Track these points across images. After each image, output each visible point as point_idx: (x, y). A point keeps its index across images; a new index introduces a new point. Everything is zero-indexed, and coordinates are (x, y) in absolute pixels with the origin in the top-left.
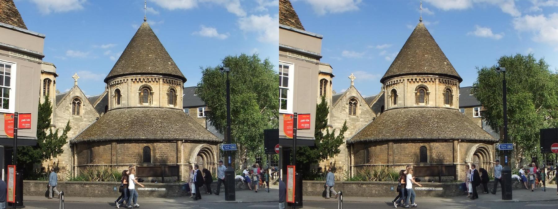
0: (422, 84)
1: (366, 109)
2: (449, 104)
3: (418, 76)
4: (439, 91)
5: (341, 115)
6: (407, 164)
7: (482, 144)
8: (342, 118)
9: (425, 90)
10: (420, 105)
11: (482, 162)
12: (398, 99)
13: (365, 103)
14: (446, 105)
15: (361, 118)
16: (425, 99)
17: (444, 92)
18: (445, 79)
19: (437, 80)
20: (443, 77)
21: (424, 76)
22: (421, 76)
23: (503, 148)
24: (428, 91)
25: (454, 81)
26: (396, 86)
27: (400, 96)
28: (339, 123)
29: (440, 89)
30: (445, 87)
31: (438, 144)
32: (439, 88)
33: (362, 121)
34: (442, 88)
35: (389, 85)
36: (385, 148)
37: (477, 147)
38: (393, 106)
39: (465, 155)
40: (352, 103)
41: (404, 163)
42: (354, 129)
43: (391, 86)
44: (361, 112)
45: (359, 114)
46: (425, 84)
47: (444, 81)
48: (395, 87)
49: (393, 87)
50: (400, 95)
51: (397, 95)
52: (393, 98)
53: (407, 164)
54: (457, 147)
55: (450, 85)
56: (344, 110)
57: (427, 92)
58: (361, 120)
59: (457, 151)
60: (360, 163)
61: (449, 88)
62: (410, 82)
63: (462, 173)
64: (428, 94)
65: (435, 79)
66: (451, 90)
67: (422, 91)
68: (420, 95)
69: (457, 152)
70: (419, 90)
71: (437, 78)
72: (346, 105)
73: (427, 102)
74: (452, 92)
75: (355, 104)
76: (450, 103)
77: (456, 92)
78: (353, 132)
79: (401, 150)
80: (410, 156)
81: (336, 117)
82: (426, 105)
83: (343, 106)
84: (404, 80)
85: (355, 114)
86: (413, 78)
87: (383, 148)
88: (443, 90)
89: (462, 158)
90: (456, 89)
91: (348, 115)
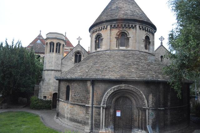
4: (110, 36)
7: (124, 85)
19: (109, 27)
28: (66, 68)
29: (113, 34)
30: (118, 32)
32: (110, 33)
34: (115, 32)
37: (114, 88)
39: (101, 97)
46: (100, 32)
47: (116, 26)
54: (89, 88)
56: (71, 60)
61: (123, 31)
64: (102, 39)
65: (107, 26)
68: (98, 42)
69: (89, 93)
74: (128, 34)
81: (64, 65)
85: (80, 60)
89: (97, 100)
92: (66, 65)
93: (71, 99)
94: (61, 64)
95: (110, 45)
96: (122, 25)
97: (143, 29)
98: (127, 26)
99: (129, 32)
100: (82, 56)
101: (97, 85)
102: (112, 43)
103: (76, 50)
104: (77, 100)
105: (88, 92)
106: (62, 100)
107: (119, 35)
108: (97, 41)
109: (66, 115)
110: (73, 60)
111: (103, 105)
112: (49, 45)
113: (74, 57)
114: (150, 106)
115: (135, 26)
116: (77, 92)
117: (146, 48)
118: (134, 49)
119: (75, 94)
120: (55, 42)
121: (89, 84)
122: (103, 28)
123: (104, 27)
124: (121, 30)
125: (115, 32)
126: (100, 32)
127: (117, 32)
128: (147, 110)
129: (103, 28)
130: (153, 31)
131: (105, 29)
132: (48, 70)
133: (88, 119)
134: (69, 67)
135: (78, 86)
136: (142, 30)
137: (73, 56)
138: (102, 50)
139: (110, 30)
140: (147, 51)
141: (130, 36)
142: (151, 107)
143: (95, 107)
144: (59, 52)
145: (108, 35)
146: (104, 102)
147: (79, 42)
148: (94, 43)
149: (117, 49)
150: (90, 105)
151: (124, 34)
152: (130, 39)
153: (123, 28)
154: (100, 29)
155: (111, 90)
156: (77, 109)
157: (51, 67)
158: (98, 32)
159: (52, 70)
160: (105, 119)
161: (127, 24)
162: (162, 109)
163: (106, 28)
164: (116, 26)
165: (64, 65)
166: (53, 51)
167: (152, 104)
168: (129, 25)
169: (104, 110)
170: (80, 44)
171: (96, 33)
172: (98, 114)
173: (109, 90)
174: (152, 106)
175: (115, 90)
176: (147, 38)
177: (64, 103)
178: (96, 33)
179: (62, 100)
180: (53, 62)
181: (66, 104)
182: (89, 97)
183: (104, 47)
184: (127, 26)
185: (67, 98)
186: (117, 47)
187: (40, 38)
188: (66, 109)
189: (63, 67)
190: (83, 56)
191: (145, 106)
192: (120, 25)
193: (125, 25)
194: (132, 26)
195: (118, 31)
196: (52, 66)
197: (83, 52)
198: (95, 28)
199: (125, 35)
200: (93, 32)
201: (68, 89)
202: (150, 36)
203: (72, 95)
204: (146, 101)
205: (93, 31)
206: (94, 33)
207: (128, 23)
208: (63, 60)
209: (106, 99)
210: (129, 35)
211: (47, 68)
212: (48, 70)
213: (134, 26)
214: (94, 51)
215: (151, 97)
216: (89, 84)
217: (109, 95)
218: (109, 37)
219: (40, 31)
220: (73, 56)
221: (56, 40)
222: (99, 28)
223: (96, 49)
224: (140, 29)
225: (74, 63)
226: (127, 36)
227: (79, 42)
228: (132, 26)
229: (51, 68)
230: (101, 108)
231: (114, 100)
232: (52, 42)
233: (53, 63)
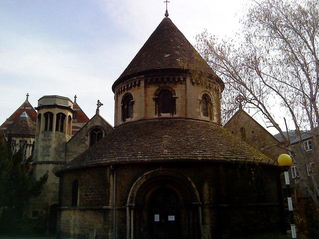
4: (146, 96)
5: (78, 148)
14: (162, 114)
17: (155, 94)
19: (142, 84)
29: (149, 93)
30: (158, 90)
32: (146, 92)
34: (152, 90)
37: (147, 175)
46: (130, 91)
47: (154, 80)
59: (109, 184)
61: (166, 88)
64: (133, 103)
66: (170, 90)
71: (142, 78)
74: (173, 93)
81: (71, 152)
93: (80, 202)
94: (66, 151)
95: (146, 111)
96: (163, 79)
97: (198, 84)
98: (171, 80)
102: (149, 108)
103: (92, 126)
105: (107, 185)
106: (66, 207)
107: (159, 95)
108: (126, 107)
109: (72, 232)
111: (130, 202)
112: (43, 118)
113: (89, 137)
114: (206, 202)
117: (206, 114)
118: (183, 116)
120: (56, 111)
121: (108, 173)
122: (133, 84)
123: (135, 83)
125: (152, 90)
126: (130, 91)
127: (155, 91)
128: (200, 208)
130: (218, 86)
131: (137, 87)
132: (41, 163)
136: (195, 85)
137: (87, 136)
138: (133, 120)
139: (145, 87)
140: (207, 119)
141: (177, 96)
142: (208, 204)
143: (119, 209)
144: (62, 130)
145: (141, 96)
146: (132, 198)
148: (120, 109)
149: (157, 116)
150: (110, 207)
152: (177, 100)
153: (165, 83)
154: (129, 86)
155: (142, 178)
156: (89, 217)
158: (126, 92)
159: (49, 163)
160: (134, 226)
162: (225, 206)
163: (139, 85)
165: (71, 152)
166: (51, 129)
167: (209, 198)
168: (174, 79)
169: (132, 212)
170: (101, 114)
173: (140, 178)
174: (209, 202)
175: (149, 177)
176: (206, 99)
177: (68, 212)
179: (66, 207)
180: (50, 147)
181: (72, 213)
182: (109, 194)
183: (136, 116)
184: (171, 80)
185: (74, 203)
186: (157, 114)
187: (26, 108)
188: (72, 221)
191: (197, 202)
192: (160, 80)
193: (168, 79)
194: (179, 79)
195: (157, 88)
197: (106, 128)
198: (122, 86)
201: (75, 185)
202: (213, 96)
203: (81, 195)
204: (197, 193)
205: (119, 90)
209: (135, 193)
211: (40, 159)
212: (41, 163)
214: (121, 123)
215: (206, 187)
217: (139, 186)
218: (143, 98)
219: (28, 96)
220: (87, 136)
221: (57, 109)
222: (128, 85)
223: (124, 119)
224: (193, 84)
226: (172, 95)
227: (98, 110)
229: (47, 159)
230: (128, 209)
231: (148, 195)
232: (49, 112)
233: (52, 150)
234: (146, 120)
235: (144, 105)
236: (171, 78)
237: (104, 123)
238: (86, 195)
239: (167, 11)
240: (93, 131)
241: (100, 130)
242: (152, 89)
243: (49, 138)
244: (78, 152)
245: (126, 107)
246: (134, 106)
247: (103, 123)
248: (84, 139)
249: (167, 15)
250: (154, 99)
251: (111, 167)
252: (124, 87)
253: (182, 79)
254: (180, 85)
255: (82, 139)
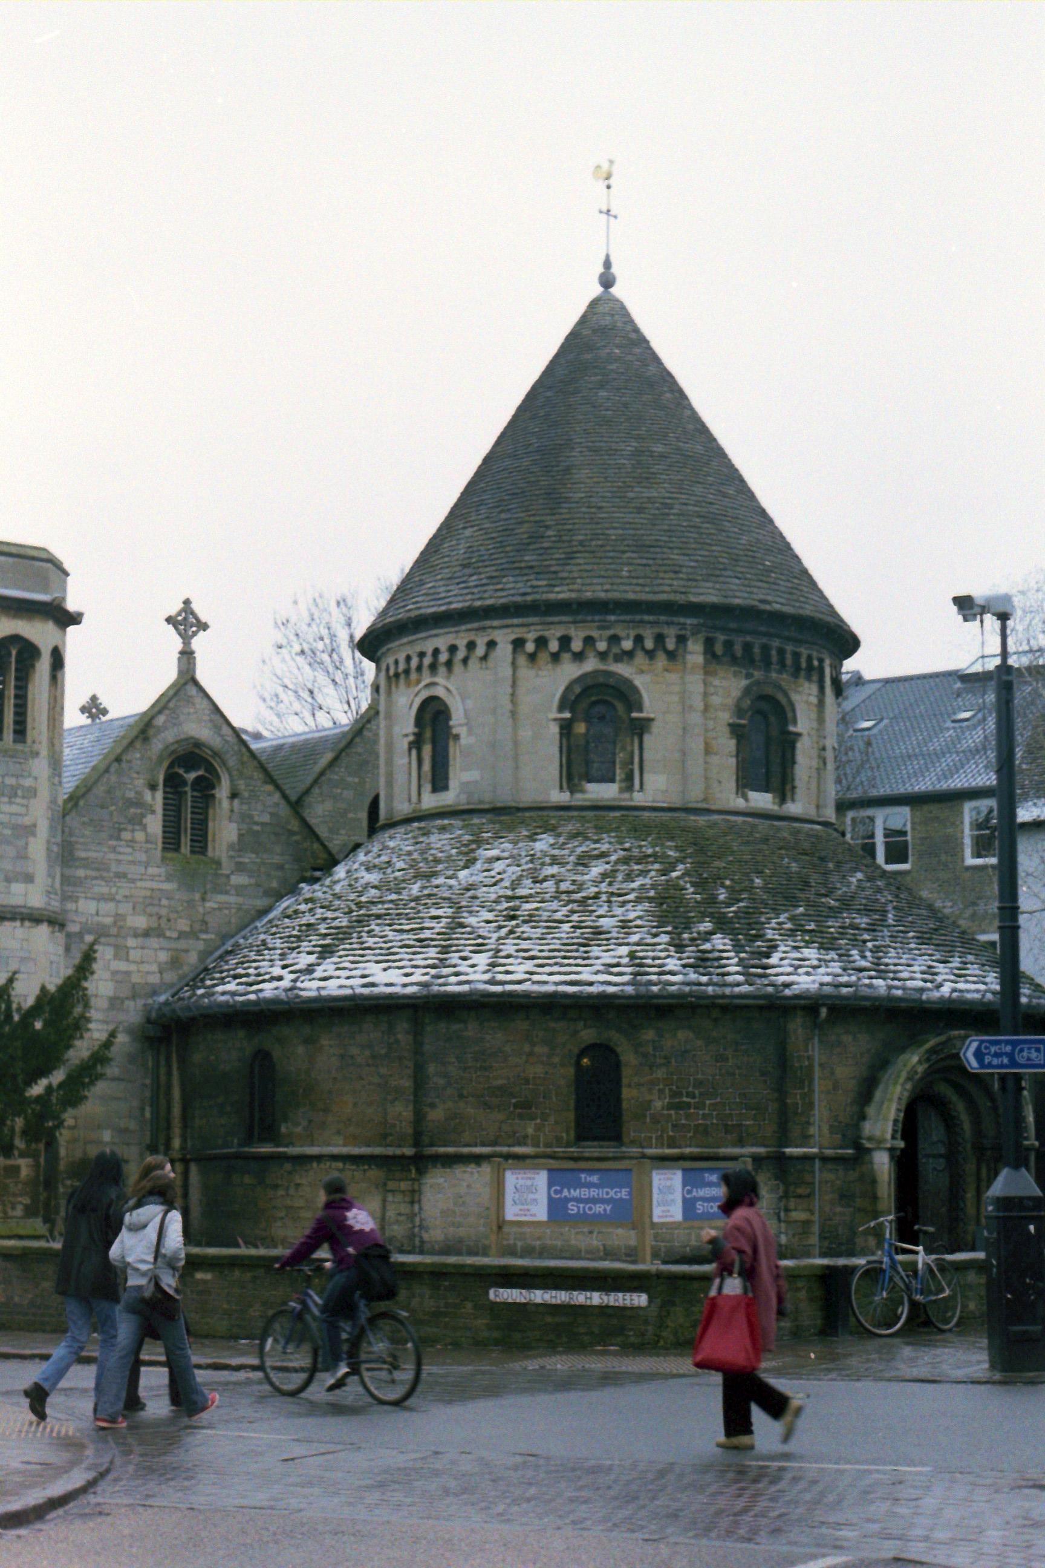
0: (602, 667)
1: (266, 818)
2: (767, 792)
3: (579, 618)
5: (114, 849)
6: (498, 1149)
8: (122, 869)
9: (620, 707)
10: (587, 796)
11: (969, 1146)
12: (455, 753)
13: (265, 782)
14: (753, 795)
15: (240, 868)
16: (621, 756)
17: (739, 712)
18: (748, 638)
20: (733, 625)
21: (613, 618)
22: (597, 618)
23: (995, 1062)
24: (641, 710)
25: (804, 652)
26: (448, 678)
27: (472, 740)
29: (716, 700)
30: (747, 691)
31: (691, 1035)
32: (706, 695)
33: (240, 890)
35: (407, 672)
36: (367, 1053)
38: (430, 801)
40: (184, 783)
41: (483, 1145)
42: (192, 934)
43: (419, 682)
44: (241, 836)
45: (224, 847)
46: (622, 669)
47: (738, 649)
48: (444, 686)
49: (427, 686)
50: (470, 733)
51: (455, 731)
52: (427, 750)
53: (498, 1149)
55: (774, 675)
57: (634, 715)
58: (238, 880)
60: (220, 1141)
61: (769, 690)
62: (532, 657)
63: (838, 1209)
64: (641, 728)
65: (681, 640)
66: (783, 701)
67: (600, 709)
68: (586, 735)
70: (583, 705)
72: (148, 796)
73: (629, 777)
74: (790, 715)
75: (206, 787)
76: (775, 782)
77: (814, 716)
78: (187, 951)
79: (465, 1069)
80: (516, 1106)
81: (86, 863)
82: (626, 795)
83: (131, 795)
84: (491, 644)
85: (201, 842)
86: (546, 634)
87: (354, 1051)
88: (730, 702)
90: (814, 700)
91: (158, 853)
92: (101, 867)
96: (765, 649)
98: (789, 660)
99: (795, 697)
100: (222, 792)
101: (833, 1038)
103: (170, 736)
104: (705, 1132)
108: (581, 728)
110: (155, 824)
111: (893, 1137)
113: (159, 795)
115: (821, 661)
116: (699, 1084)
118: (812, 813)
119: (680, 1094)
122: (649, 644)
123: (660, 639)
124: (758, 683)
126: (622, 669)
127: (736, 693)
129: (649, 644)
131: (661, 660)
133: (807, 1223)
134: (123, 889)
135: (700, 1043)
138: (638, 798)
147: (187, 656)
149: (740, 803)
151: (764, 706)
152: (799, 745)
154: (627, 645)
157: (17, 888)
161: (789, 648)
164: (738, 649)
165: (86, 863)
168: (797, 655)
170: (201, 676)
171: (569, 671)
172: (842, 1196)
178: (569, 671)
180: (30, 830)
184: (789, 660)
189: (77, 882)
190: (234, 795)
192: (757, 650)
193: (781, 652)
194: (810, 658)
196: (29, 879)
199: (772, 719)
200: (532, 657)
205: (542, 642)
206: (543, 657)
207: (798, 642)
208: (73, 820)
210: (795, 723)
213: (816, 663)
216: (797, 1026)
218: (695, 718)
220: (153, 787)
221: (50, 626)
222: (614, 639)
225: (163, 859)
227: (187, 656)
228: (810, 658)
234: (709, 811)
235: (702, 747)
236: (789, 648)
237: (226, 730)
238: (670, 1107)
239: (607, 264)
240: (171, 766)
241: (210, 768)
242: (725, 683)
243: (28, 782)
244: (114, 868)
245: (581, 728)
246: (646, 738)
247: (217, 728)
248: (139, 803)
249: (607, 281)
250: (736, 730)
251: (824, 1012)
252: (589, 641)
253: (816, 663)
254: (807, 685)
255: (130, 803)
